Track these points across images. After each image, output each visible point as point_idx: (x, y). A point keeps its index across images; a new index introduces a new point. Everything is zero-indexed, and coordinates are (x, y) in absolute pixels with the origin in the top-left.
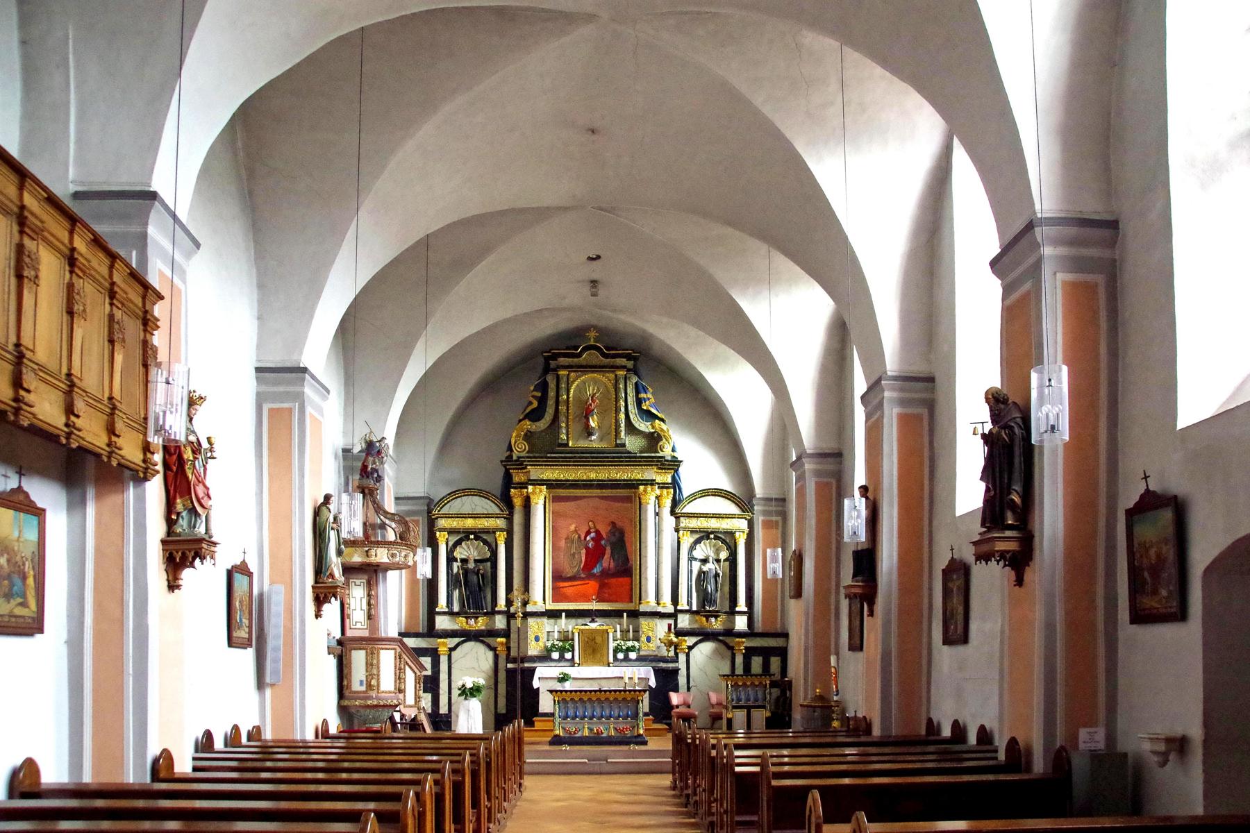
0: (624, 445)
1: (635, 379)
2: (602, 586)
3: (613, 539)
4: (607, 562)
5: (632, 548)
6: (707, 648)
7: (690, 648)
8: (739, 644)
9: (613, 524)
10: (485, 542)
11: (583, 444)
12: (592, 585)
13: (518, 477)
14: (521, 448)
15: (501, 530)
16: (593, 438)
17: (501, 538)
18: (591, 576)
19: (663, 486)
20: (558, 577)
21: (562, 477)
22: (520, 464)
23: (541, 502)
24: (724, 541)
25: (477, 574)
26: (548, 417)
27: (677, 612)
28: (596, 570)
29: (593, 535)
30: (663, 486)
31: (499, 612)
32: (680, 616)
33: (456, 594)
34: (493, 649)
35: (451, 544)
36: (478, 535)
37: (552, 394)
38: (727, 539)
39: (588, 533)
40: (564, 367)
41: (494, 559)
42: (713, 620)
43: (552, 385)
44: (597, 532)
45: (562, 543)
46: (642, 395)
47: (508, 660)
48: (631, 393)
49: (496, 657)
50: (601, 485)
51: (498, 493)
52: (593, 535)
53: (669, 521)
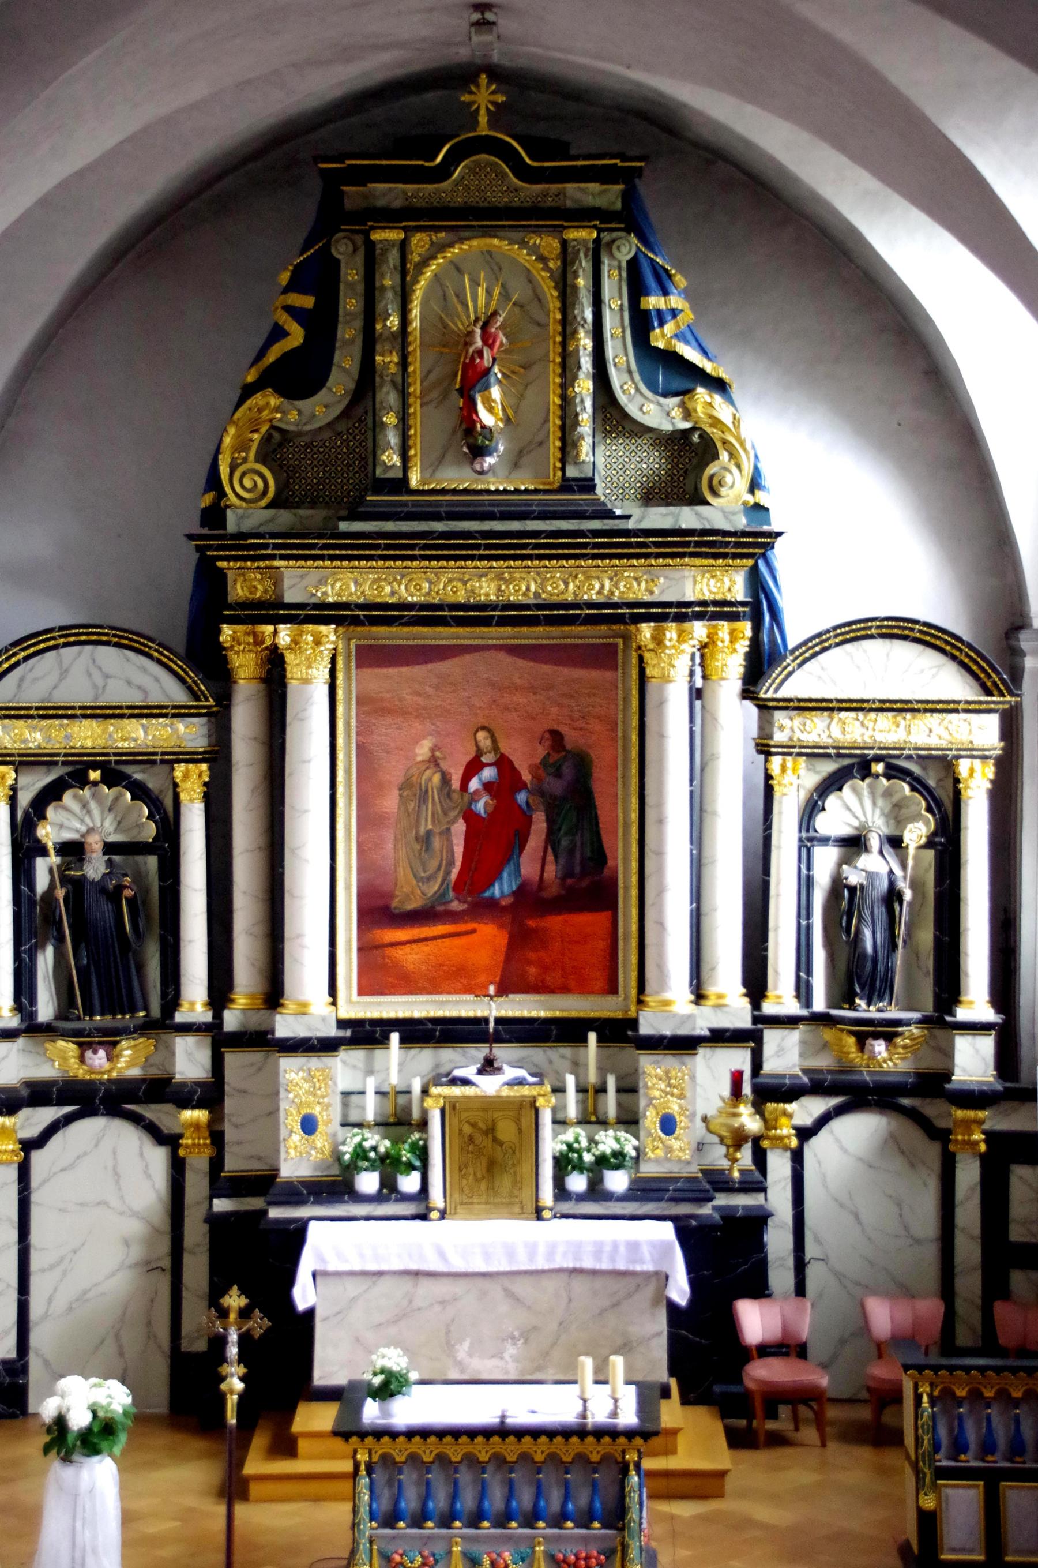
0: (587, 485)
1: (627, 248)
2: (520, 941)
3: (556, 786)
4: (533, 862)
6: (858, 1132)
7: (805, 1134)
8: (968, 1125)
9: (556, 737)
10: (140, 792)
11: (456, 477)
12: (488, 939)
13: (244, 585)
14: (249, 492)
15: (191, 758)
16: (489, 461)
17: (192, 783)
18: (484, 908)
19: (719, 611)
20: (377, 911)
21: (386, 593)
22: (248, 547)
23: (321, 674)
24: (918, 785)
25: (114, 896)
26: (340, 384)
27: (763, 1020)
28: (502, 889)
29: (488, 773)
30: (719, 611)
31: (186, 1028)
32: (772, 1037)
33: (46, 960)
34: (168, 1140)
35: (24, 799)
36: (115, 770)
37: (350, 304)
38: (933, 783)
39: (474, 767)
40: (390, 217)
41: (168, 844)
42: (880, 1047)
43: (351, 274)
44: (503, 764)
45: (390, 803)
46: (653, 302)
47: (221, 1183)
48: (615, 298)
49: (177, 1168)
50: (514, 615)
51: (177, 630)
52: (488, 773)
53: (734, 718)
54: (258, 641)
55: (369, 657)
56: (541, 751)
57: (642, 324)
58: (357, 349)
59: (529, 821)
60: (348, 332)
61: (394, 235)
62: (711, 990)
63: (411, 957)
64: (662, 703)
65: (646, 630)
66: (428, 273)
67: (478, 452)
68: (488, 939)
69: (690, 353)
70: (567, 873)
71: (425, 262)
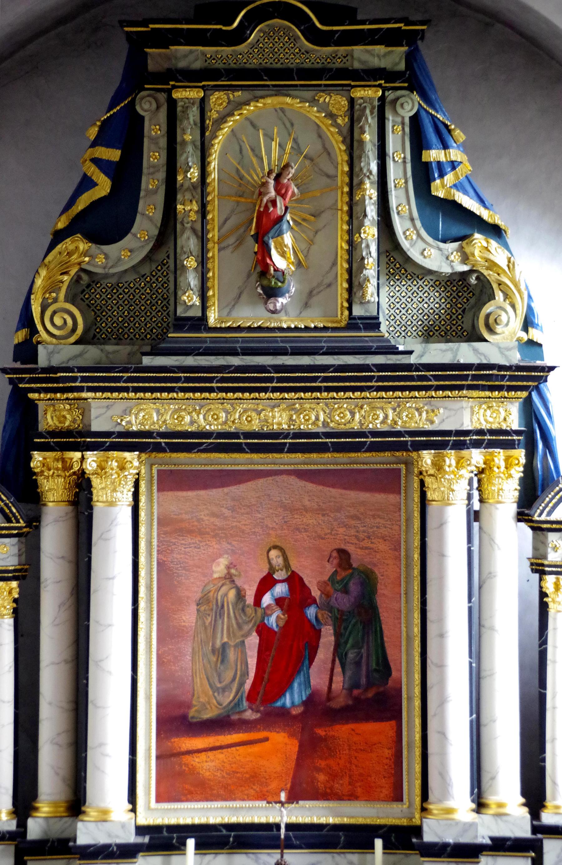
0: (372, 323)
2: (310, 748)
3: (344, 602)
4: (322, 673)
5: (401, 631)
9: (343, 555)
11: (251, 315)
12: (278, 748)
13: (53, 415)
16: (282, 301)
18: (277, 718)
19: (496, 439)
20: (175, 720)
22: (57, 380)
23: (125, 497)
28: (293, 698)
29: (281, 589)
30: (496, 439)
37: (154, 157)
39: (267, 583)
40: (192, 77)
43: (154, 129)
44: (294, 580)
45: (189, 617)
46: (434, 155)
52: (281, 589)
54: (67, 467)
55: (169, 481)
56: (330, 569)
57: (423, 174)
58: (160, 198)
59: (318, 634)
60: (152, 183)
61: (196, 94)
62: (491, 799)
63: (207, 765)
64: (441, 525)
65: (427, 457)
66: (226, 129)
67: (271, 293)
68: (278, 748)
69: (468, 202)
70: (355, 685)
71: (222, 120)
